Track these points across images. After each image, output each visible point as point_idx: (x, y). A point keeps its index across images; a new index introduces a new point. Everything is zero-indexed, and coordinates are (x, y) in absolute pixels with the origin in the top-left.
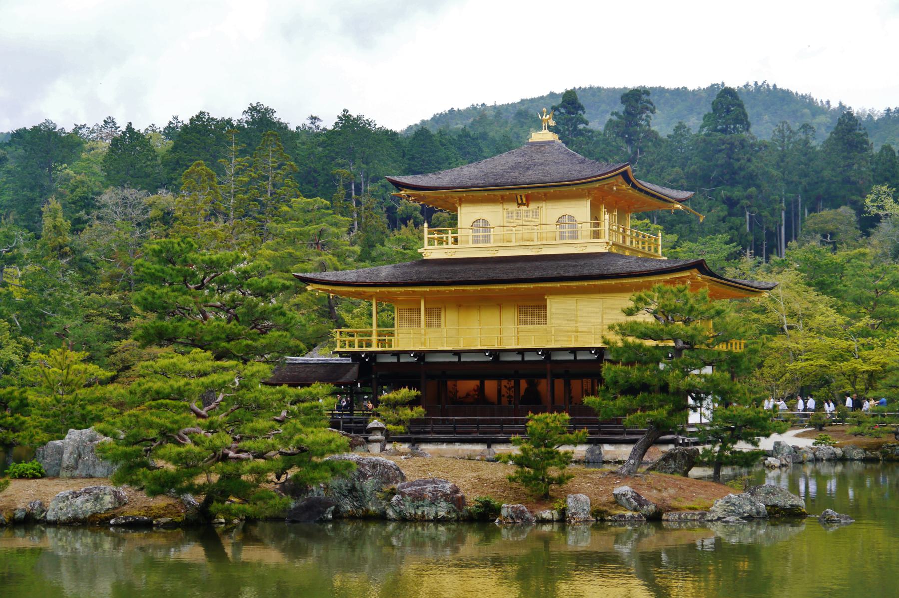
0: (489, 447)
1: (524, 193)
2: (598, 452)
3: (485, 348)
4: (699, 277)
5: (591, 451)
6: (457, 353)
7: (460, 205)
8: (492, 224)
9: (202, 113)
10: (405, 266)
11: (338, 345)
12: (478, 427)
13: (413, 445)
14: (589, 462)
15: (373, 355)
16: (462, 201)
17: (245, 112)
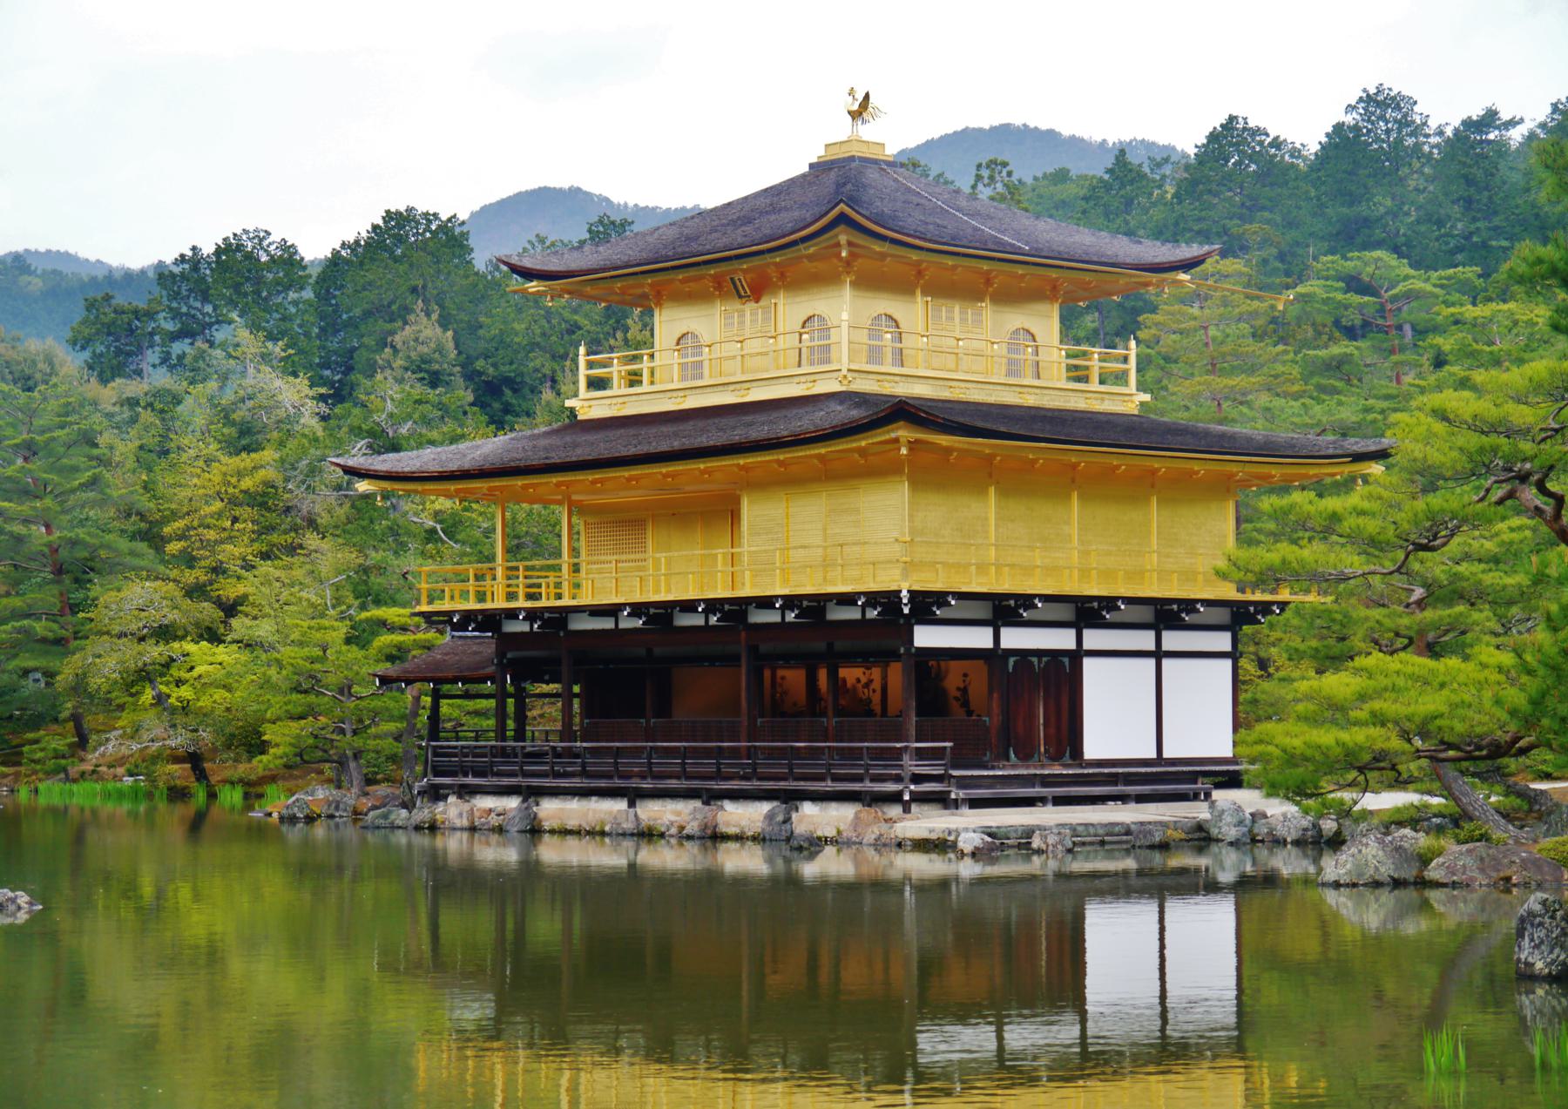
0: (632, 804)
1: (742, 272)
2: (780, 818)
3: (622, 601)
4: (944, 440)
5: (770, 817)
6: (612, 611)
7: (659, 304)
8: (706, 338)
9: (1232, 118)
10: (538, 436)
11: (424, 599)
12: (791, 767)
13: (524, 801)
14: (764, 840)
15: (489, 621)
16: (660, 297)
17: (1350, 108)
